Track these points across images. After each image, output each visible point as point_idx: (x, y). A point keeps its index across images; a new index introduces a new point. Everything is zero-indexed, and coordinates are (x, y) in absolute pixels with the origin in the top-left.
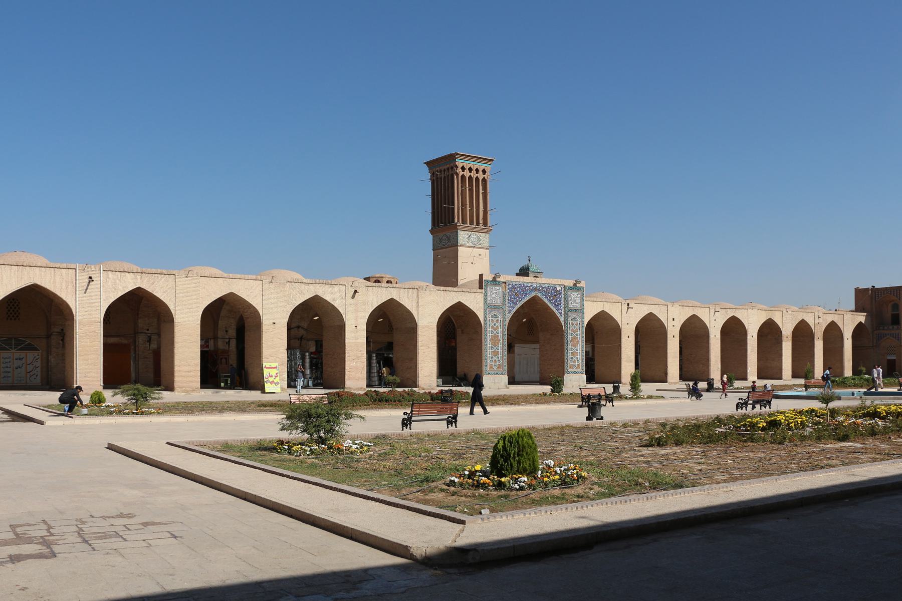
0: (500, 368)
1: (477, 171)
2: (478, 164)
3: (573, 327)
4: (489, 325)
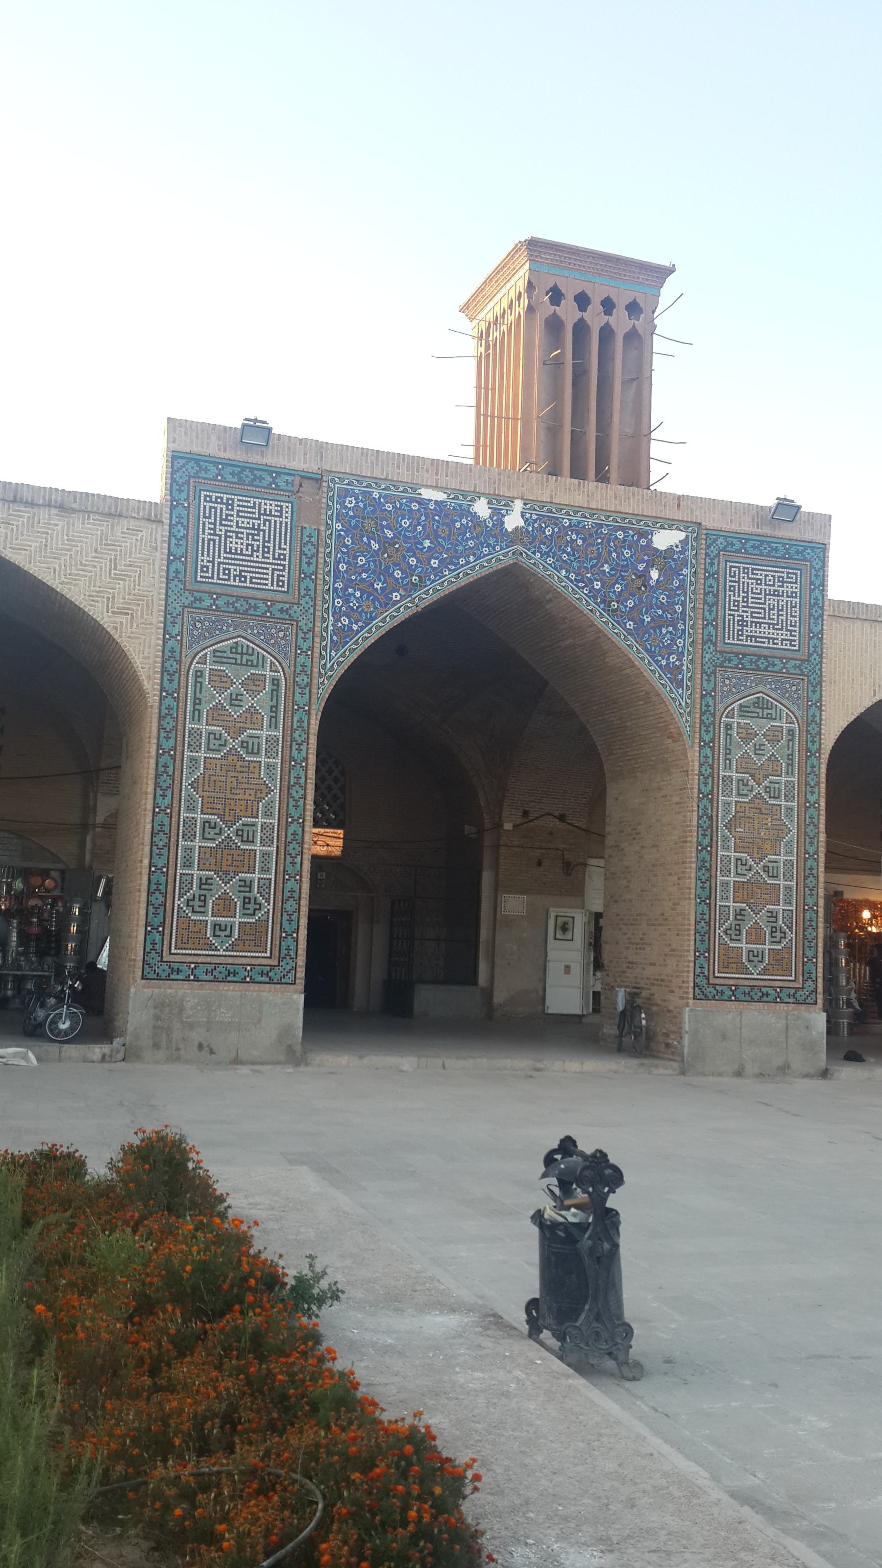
0: (260, 945)
1: (608, 305)
2: (612, 283)
3: (749, 748)
4: (197, 701)
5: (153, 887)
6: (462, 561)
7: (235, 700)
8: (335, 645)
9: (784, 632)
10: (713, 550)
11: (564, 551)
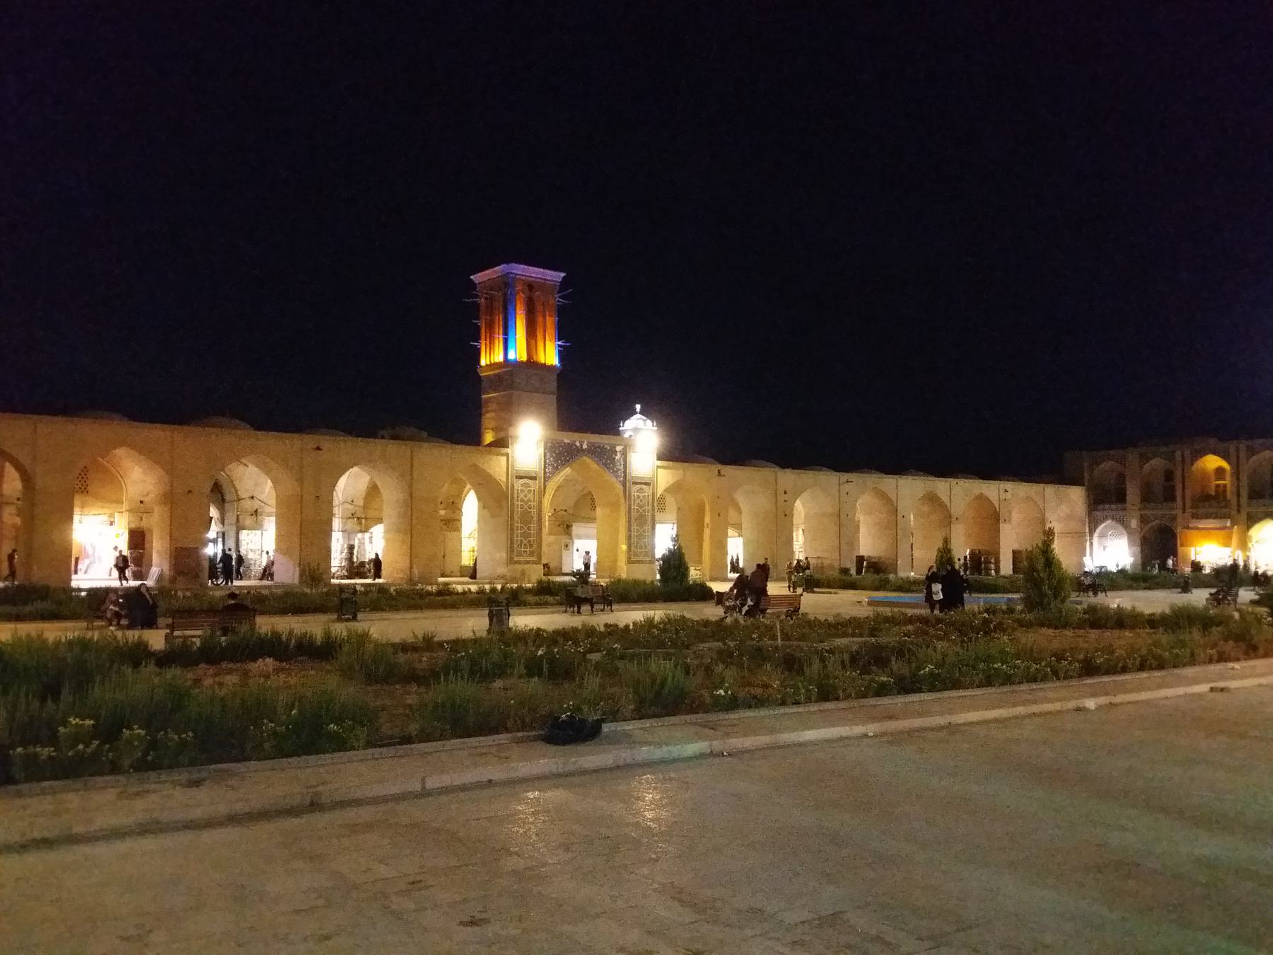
4: (518, 497)
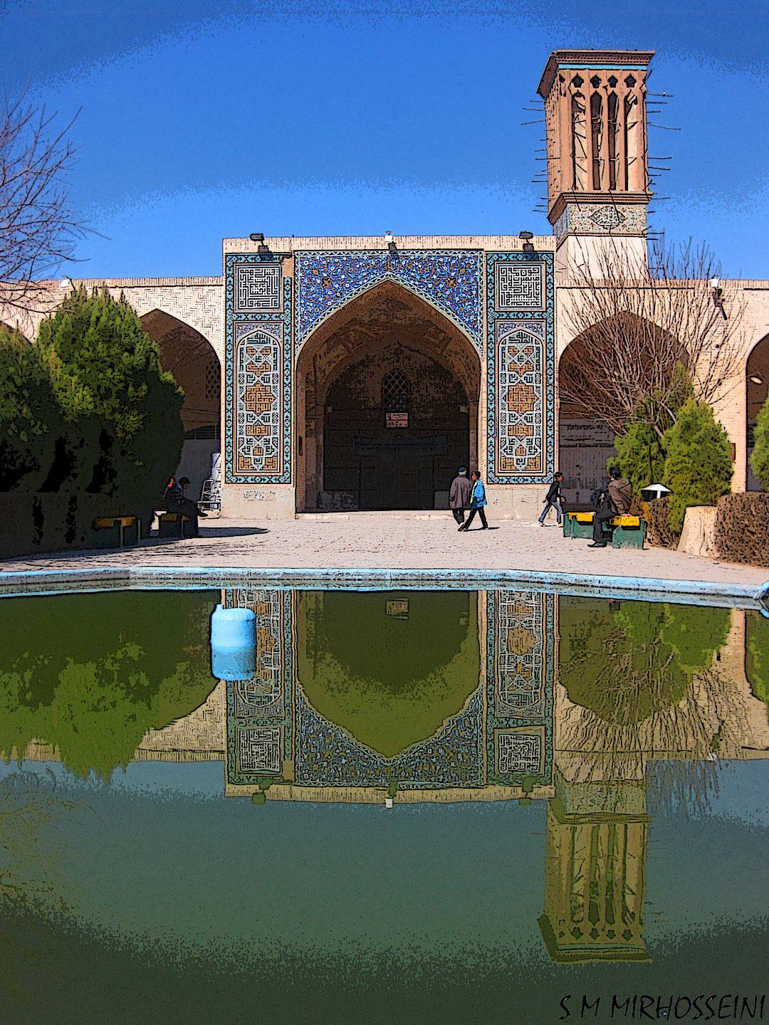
4: (242, 361)
5: (227, 444)
6: (361, 283)
7: (258, 360)
8: (302, 330)
9: (533, 298)
10: (491, 262)
11: (412, 272)
